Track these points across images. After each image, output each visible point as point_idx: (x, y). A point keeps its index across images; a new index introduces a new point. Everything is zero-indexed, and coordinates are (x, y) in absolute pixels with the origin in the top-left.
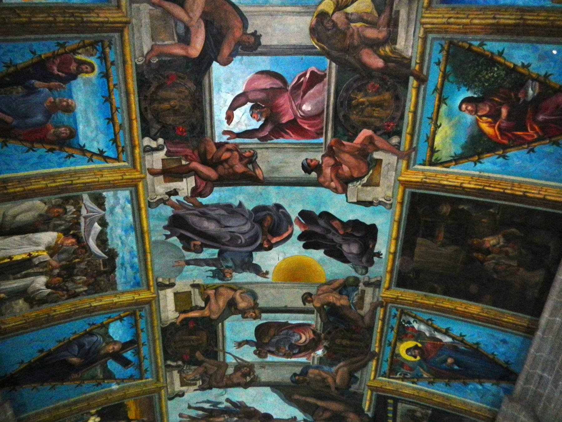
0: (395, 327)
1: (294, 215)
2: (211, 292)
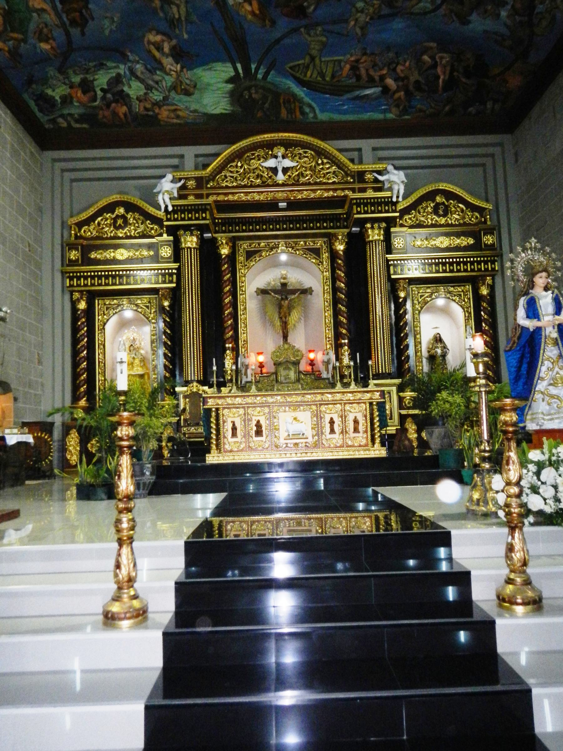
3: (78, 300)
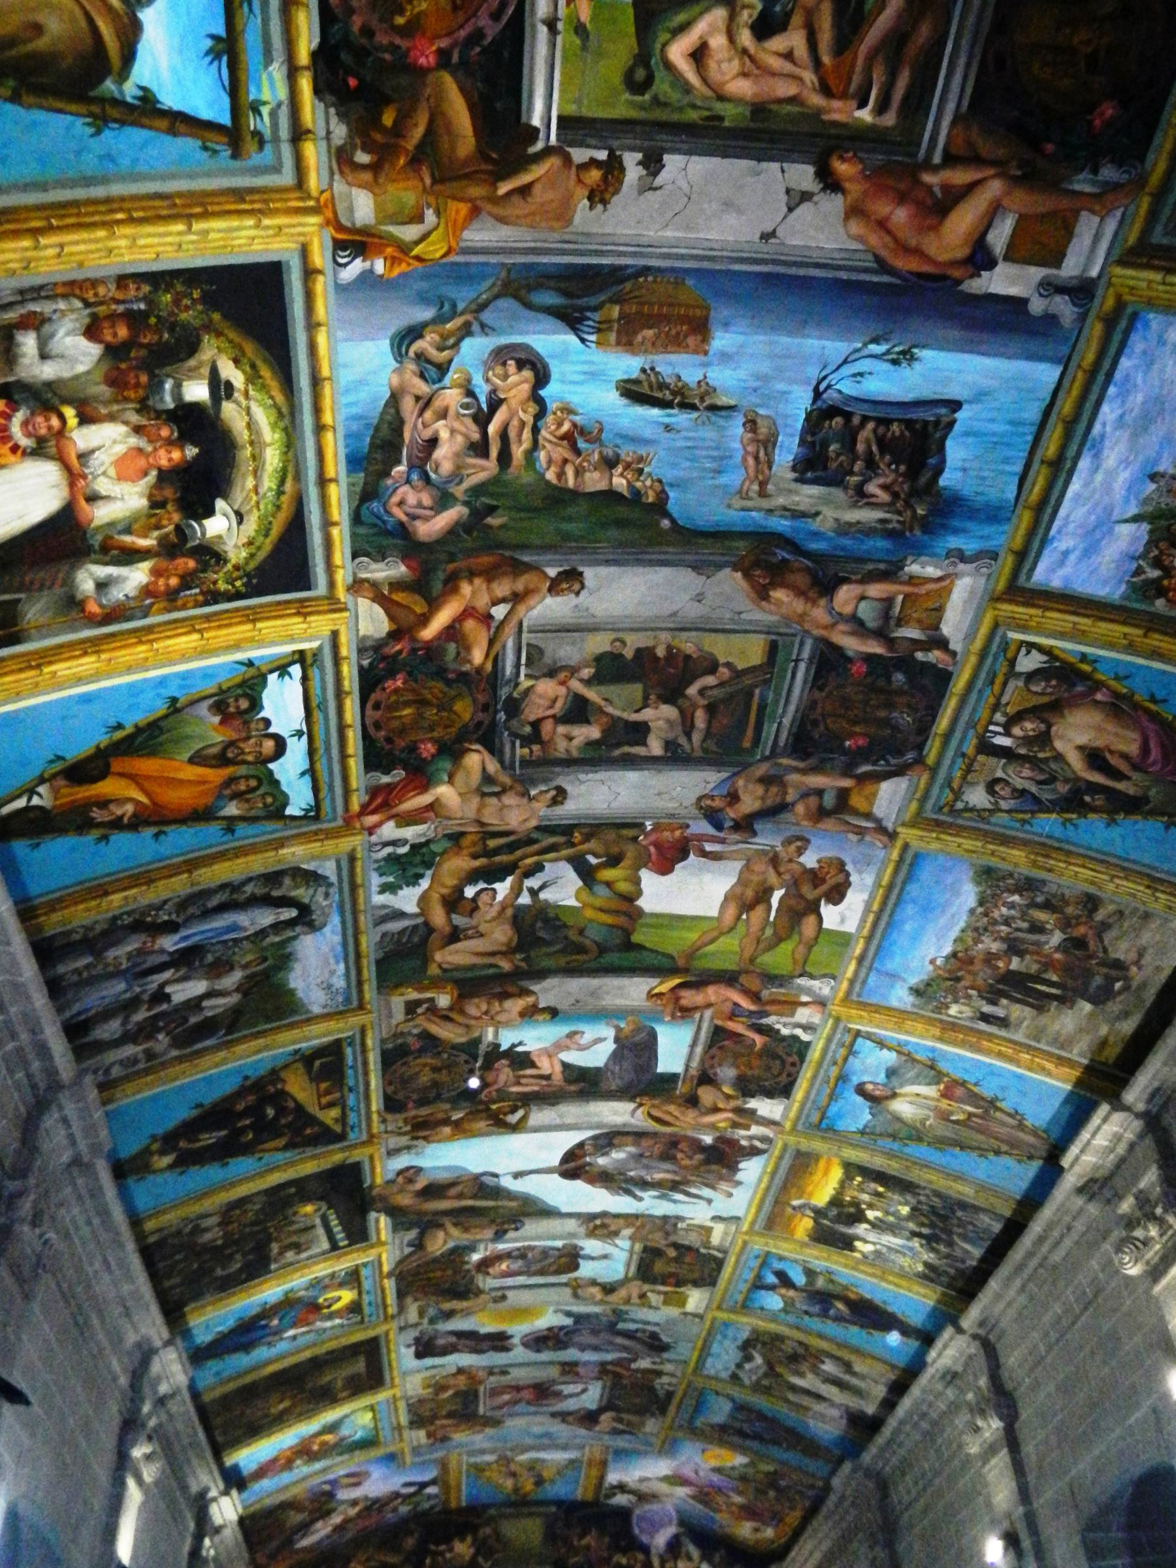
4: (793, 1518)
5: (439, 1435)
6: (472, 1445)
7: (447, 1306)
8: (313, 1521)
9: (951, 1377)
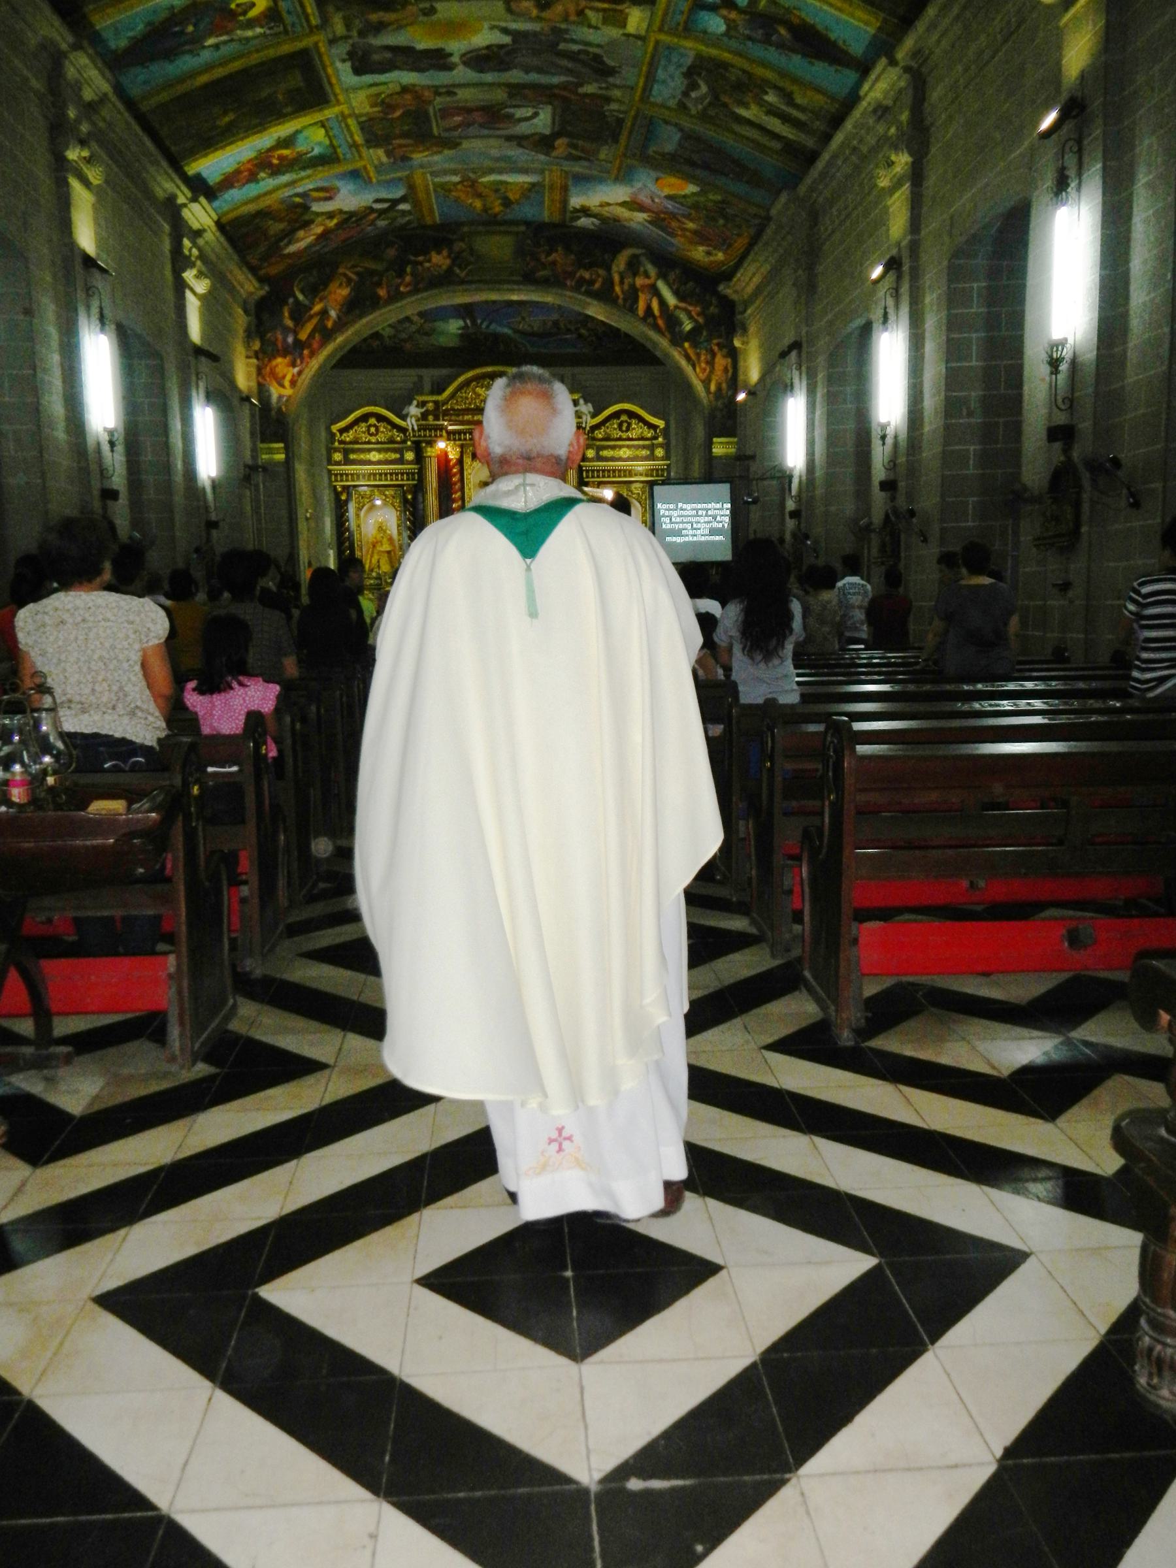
0: (285, 15)
1: (461, 68)
2: (573, 18)
3: (341, 493)
4: (740, 243)
5: (399, 152)
6: (433, 167)
7: (374, 17)
8: (293, 231)
9: (882, 111)
